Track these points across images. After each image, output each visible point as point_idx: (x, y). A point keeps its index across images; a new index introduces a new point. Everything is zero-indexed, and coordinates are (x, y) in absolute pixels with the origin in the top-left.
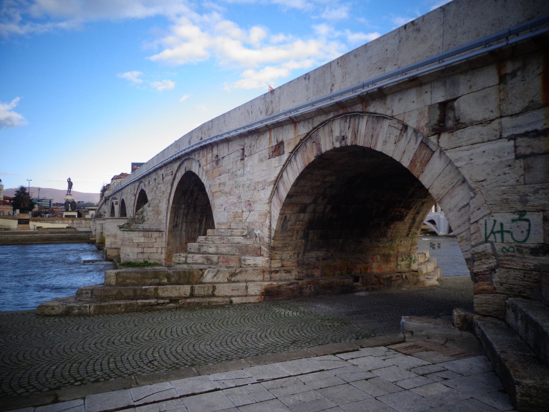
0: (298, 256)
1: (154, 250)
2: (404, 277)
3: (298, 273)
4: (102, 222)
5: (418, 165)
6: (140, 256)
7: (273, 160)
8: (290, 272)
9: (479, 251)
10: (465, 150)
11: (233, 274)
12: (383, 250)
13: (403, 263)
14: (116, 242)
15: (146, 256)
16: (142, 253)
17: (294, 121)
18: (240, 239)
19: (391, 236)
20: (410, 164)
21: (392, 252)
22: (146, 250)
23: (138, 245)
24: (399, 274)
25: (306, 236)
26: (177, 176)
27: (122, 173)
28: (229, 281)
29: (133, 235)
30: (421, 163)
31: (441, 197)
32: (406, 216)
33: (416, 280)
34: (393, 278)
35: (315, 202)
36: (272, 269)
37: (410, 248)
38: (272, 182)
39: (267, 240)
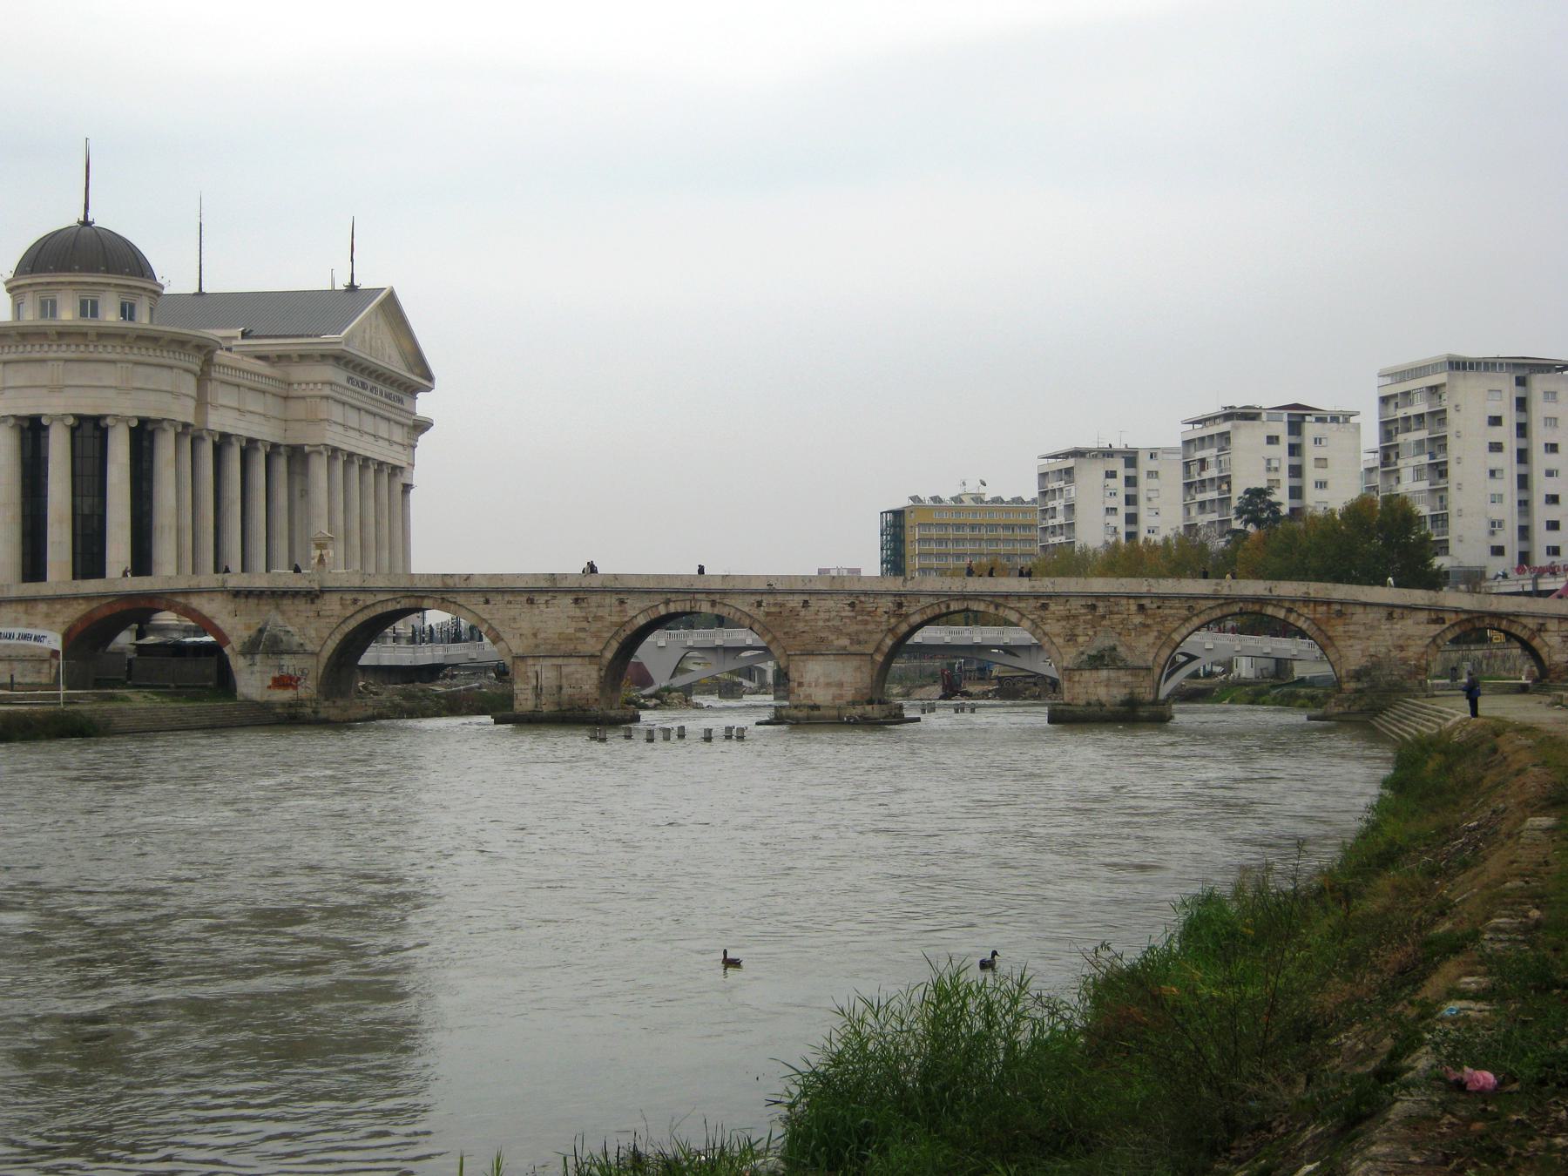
14: (841, 696)
23: (1125, 685)
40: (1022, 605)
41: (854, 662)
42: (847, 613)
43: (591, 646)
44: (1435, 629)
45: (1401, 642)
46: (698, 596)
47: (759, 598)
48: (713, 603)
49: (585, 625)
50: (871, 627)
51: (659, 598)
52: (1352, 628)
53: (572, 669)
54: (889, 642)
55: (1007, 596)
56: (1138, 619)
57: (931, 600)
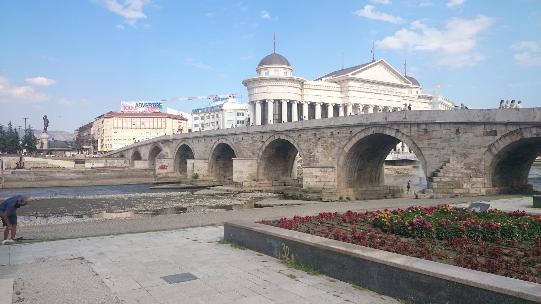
1: (329, 180)
4: (193, 161)
6: (318, 183)
11: (473, 185)
14: (242, 177)
15: (323, 183)
16: (320, 181)
17: (506, 124)
18: (464, 171)
22: (322, 180)
23: (317, 177)
25: (495, 169)
26: (359, 134)
27: (111, 112)
28: (472, 188)
29: (312, 170)
40: (294, 135)
41: (249, 162)
42: (251, 142)
43: (207, 156)
44: (490, 140)
45: (464, 151)
46: (224, 137)
47: (233, 137)
48: (226, 139)
49: (205, 149)
50: (256, 148)
51: (217, 138)
52: (432, 141)
53: (197, 164)
54: (261, 154)
55: (289, 131)
56: (330, 141)
57: (270, 135)
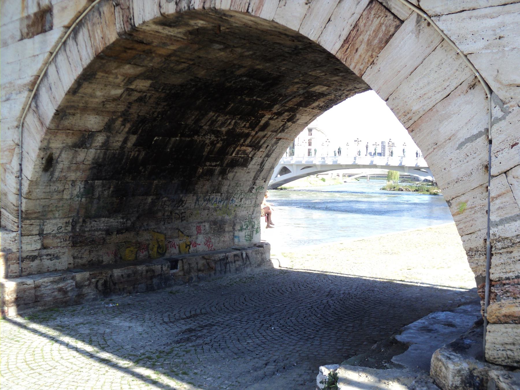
0: (74, 227)
2: (244, 255)
3: (74, 258)
5: (362, 49)
7: (28, 42)
8: (57, 258)
9: (508, 235)
10: (485, 16)
12: (215, 214)
13: (242, 234)
19: (228, 192)
20: (342, 46)
21: (227, 217)
24: (237, 252)
30: (369, 43)
31: (415, 118)
32: (252, 158)
33: (260, 259)
34: (229, 259)
35: (108, 128)
36: (24, 255)
37: (252, 209)
38: (25, 85)
39: (12, 198)
